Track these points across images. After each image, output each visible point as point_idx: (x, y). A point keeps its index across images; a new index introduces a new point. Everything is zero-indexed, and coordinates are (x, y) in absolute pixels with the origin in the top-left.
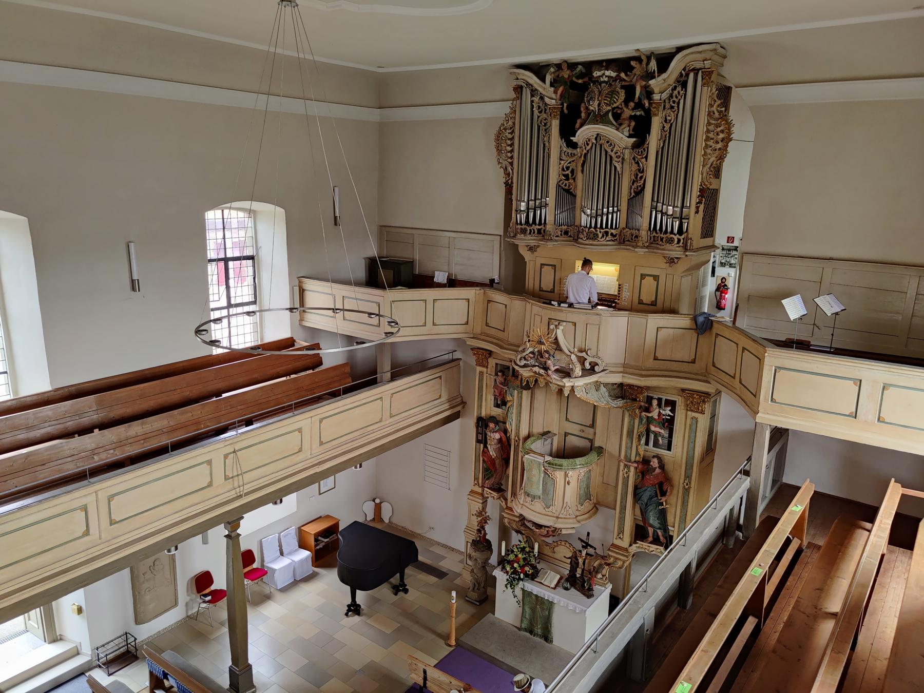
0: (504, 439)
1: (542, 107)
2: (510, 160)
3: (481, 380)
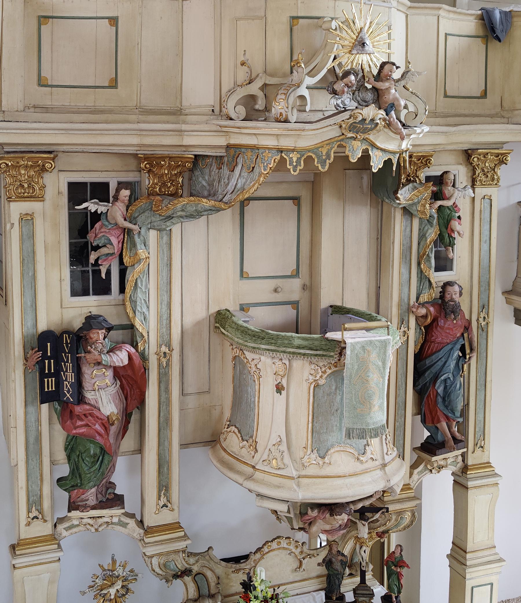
0: (137, 360)
3: (28, 237)
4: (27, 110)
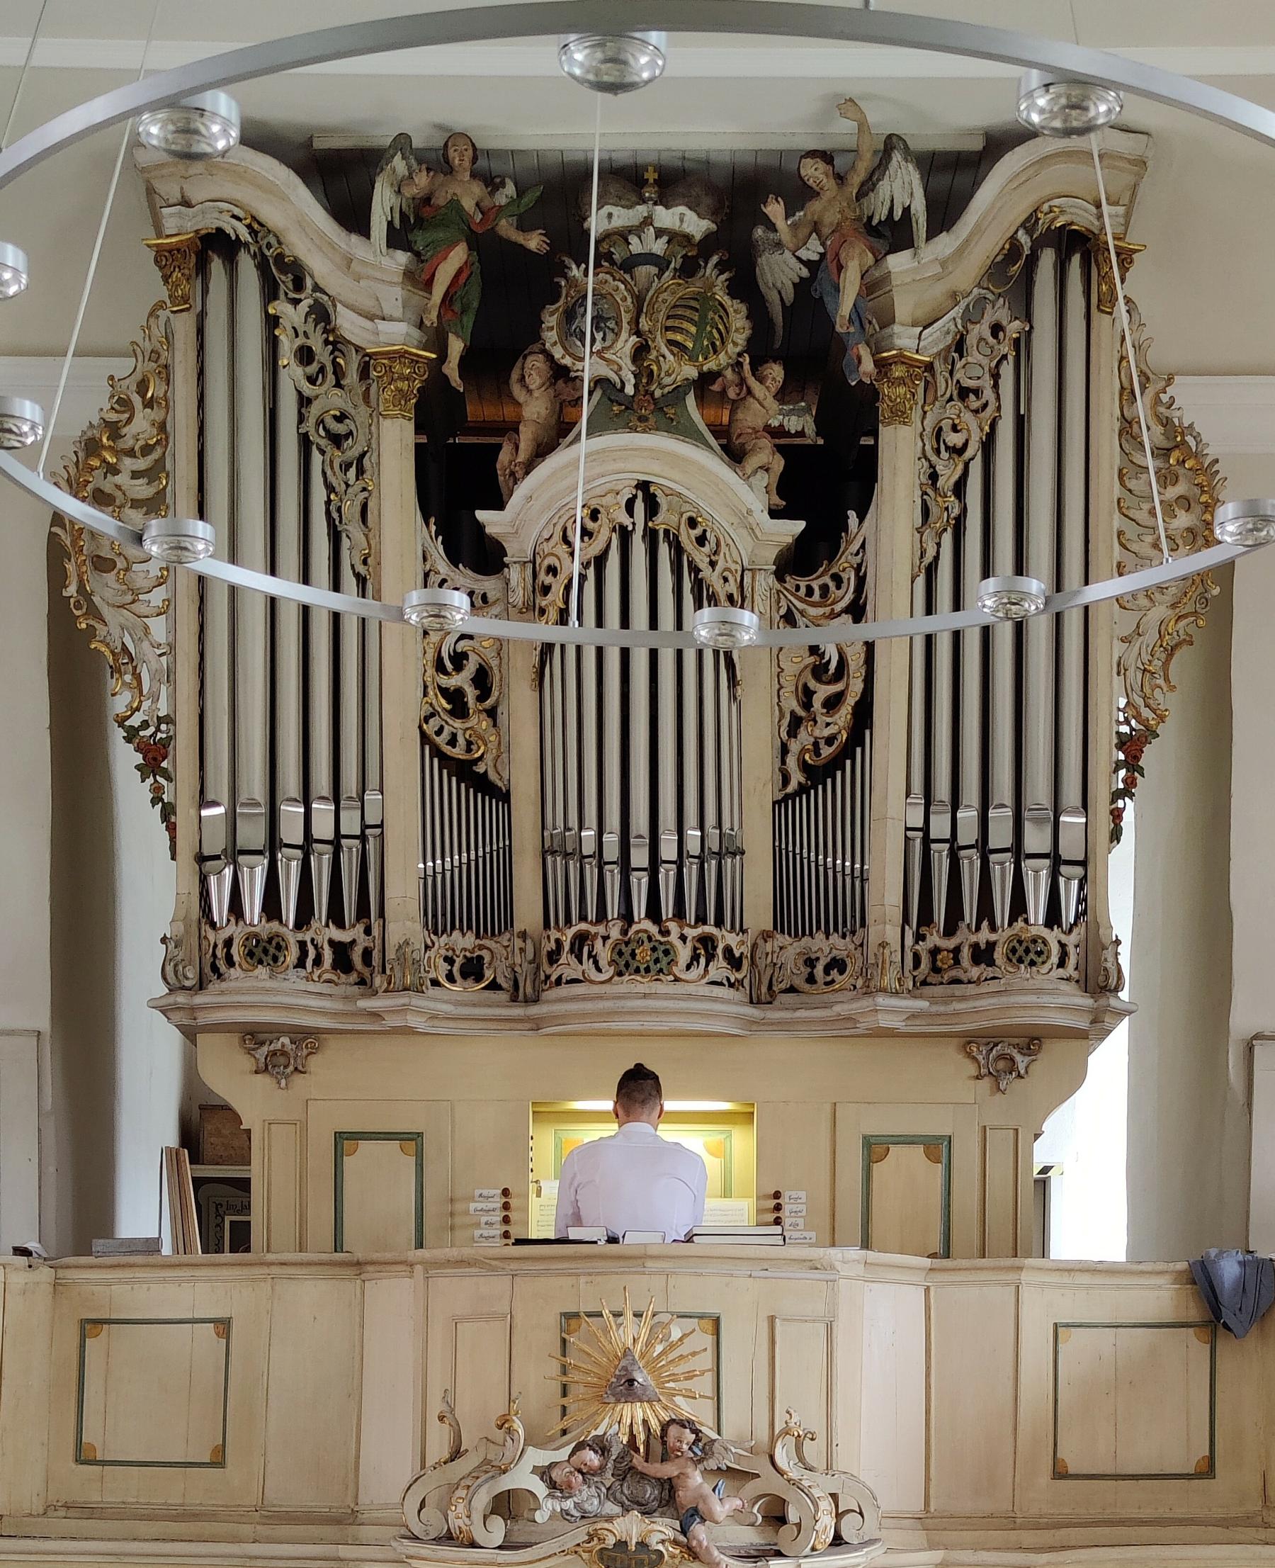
1: (323, 354)
4: (50, 1513)
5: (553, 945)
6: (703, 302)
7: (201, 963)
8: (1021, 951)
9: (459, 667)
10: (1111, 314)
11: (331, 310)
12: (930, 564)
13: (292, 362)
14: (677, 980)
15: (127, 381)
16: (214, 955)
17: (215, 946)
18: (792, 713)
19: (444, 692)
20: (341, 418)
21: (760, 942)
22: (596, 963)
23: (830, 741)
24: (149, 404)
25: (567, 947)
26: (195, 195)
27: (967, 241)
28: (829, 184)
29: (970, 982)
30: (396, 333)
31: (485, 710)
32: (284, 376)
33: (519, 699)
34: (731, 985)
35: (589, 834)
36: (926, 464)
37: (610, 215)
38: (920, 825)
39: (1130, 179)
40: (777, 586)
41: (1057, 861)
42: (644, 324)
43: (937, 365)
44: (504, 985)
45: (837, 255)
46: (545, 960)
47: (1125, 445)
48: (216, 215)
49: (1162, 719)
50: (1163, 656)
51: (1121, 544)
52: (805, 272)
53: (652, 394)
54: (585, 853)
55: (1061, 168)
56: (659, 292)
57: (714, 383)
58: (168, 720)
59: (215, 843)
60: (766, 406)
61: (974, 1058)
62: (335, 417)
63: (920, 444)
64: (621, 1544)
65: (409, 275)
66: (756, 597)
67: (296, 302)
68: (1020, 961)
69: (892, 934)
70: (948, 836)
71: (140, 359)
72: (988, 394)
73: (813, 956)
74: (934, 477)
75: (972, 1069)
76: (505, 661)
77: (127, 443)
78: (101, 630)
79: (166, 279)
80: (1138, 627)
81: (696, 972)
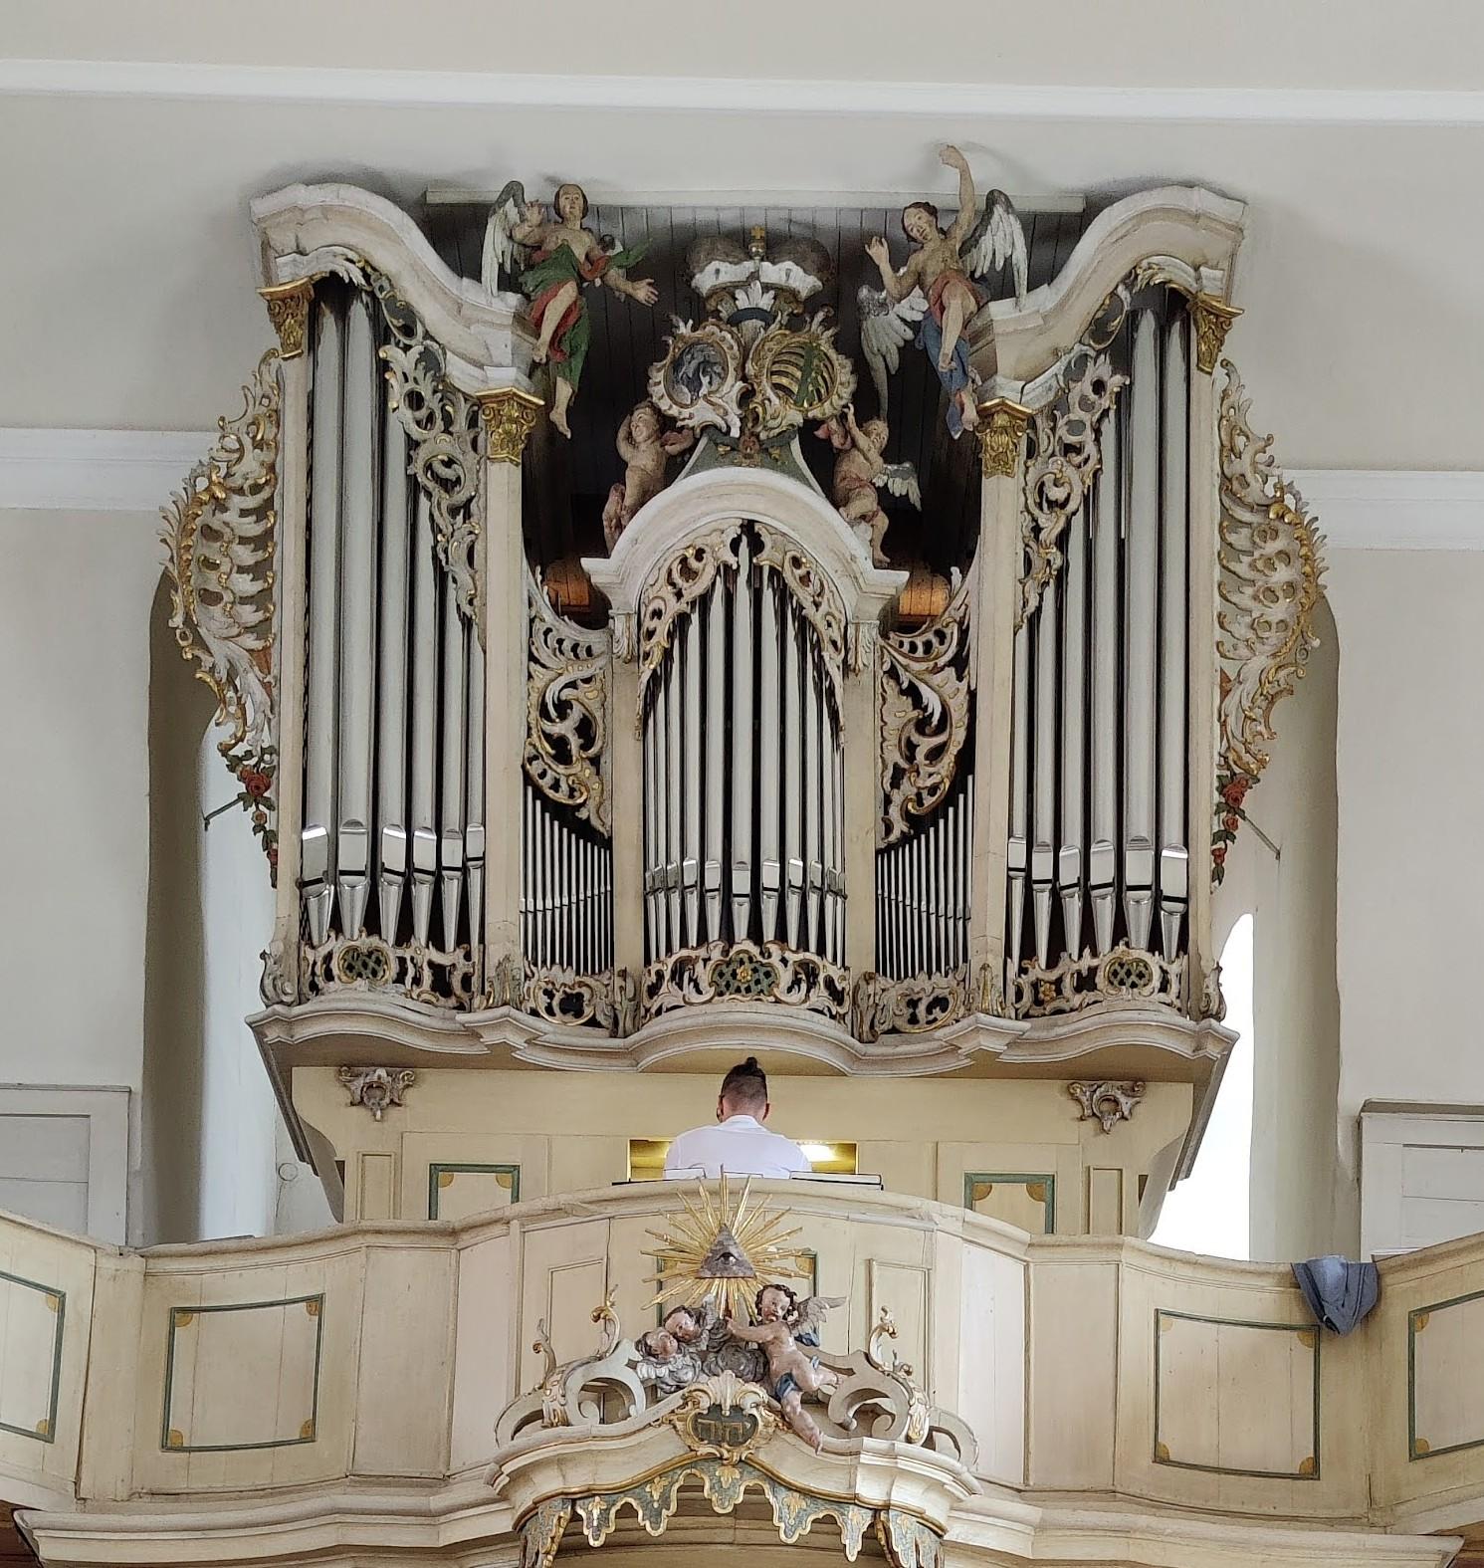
1: (432, 402)
2: (251, 642)
5: (654, 978)
6: (809, 351)
7: (298, 978)
8: (1122, 973)
9: (563, 716)
10: (1210, 374)
11: (441, 358)
12: (1033, 614)
13: (402, 405)
14: (778, 1001)
15: (237, 424)
16: (313, 974)
17: (315, 963)
18: (896, 766)
19: (548, 737)
20: (449, 463)
21: (862, 983)
22: (697, 986)
23: (933, 790)
24: (258, 445)
25: (667, 976)
26: (307, 244)
27: (1068, 295)
28: (932, 234)
29: (1072, 1010)
30: (506, 377)
31: (588, 758)
32: (393, 419)
33: (623, 750)
34: (833, 1017)
35: (691, 862)
36: (1029, 518)
37: (718, 271)
38: (1023, 865)
39: (1228, 245)
40: (881, 641)
41: (1159, 898)
42: (750, 368)
43: (1039, 421)
44: (604, 1023)
45: (940, 296)
46: (645, 995)
47: (1224, 497)
48: (331, 258)
49: (1262, 764)
50: (1264, 704)
51: (1223, 596)
52: (909, 334)
53: (758, 436)
54: (686, 884)
55: (1156, 225)
56: (765, 340)
57: (817, 429)
58: (273, 750)
59: (316, 867)
60: (868, 455)
61: (1078, 1100)
62: (443, 462)
63: (1023, 498)
64: (716, 1408)
65: (519, 318)
66: (860, 649)
67: (407, 348)
68: (1122, 983)
69: (996, 962)
70: (1050, 877)
71: (251, 402)
72: (1090, 448)
73: (916, 997)
74: (1037, 530)
75: (1076, 1111)
76: (609, 711)
77: (237, 481)
78: (207, 661)
79: (278, 329)
80: (1239, 675)
81: (797, 996)
